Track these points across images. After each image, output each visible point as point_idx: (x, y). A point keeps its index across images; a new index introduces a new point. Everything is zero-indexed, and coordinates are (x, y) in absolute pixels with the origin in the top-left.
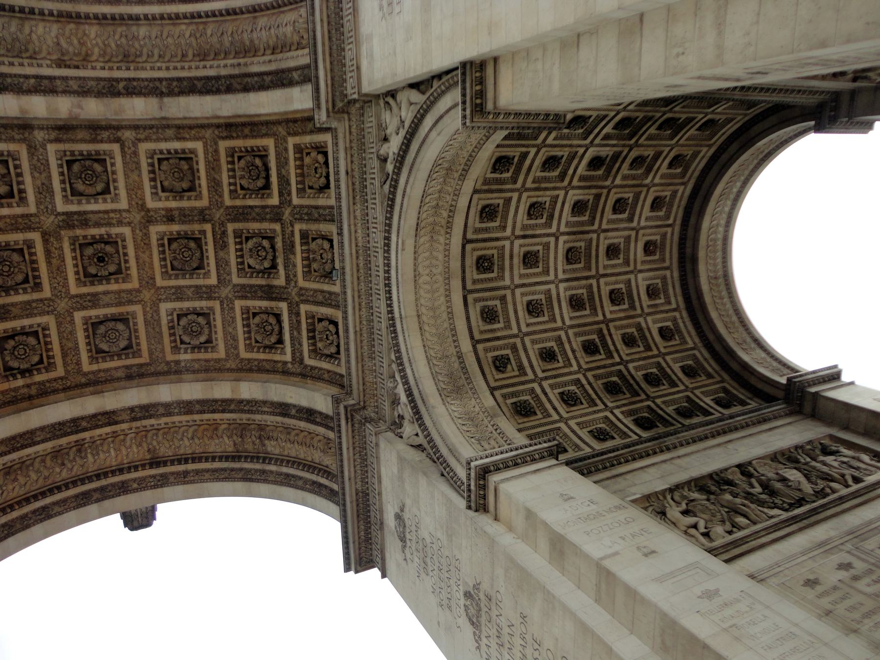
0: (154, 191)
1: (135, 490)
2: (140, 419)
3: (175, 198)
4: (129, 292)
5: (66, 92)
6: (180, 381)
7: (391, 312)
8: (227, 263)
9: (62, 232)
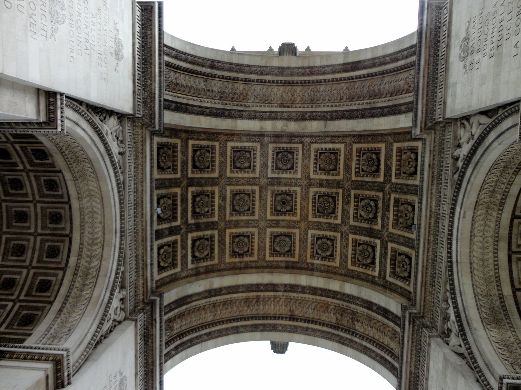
0: (315, 169)
1: (280, 331)
2: (289, 291)
3: (325, 175)
4: (294, 221)
6: (312, 275)
7: (450, 257)
8: (348, 212)
9: (268, 187)
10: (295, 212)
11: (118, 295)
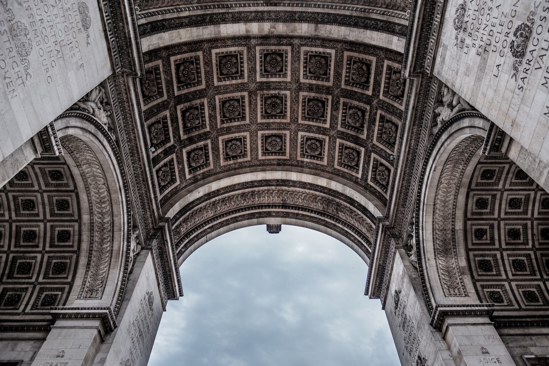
0: (305, 73)
1: (274, 216)
2: (281, 186)
4: (285, 124)
5: (269, 20)
7: (419, 196)
8: (337, 118)
9: (258, 92)
10: (285, 73)
11: (133, 237)
